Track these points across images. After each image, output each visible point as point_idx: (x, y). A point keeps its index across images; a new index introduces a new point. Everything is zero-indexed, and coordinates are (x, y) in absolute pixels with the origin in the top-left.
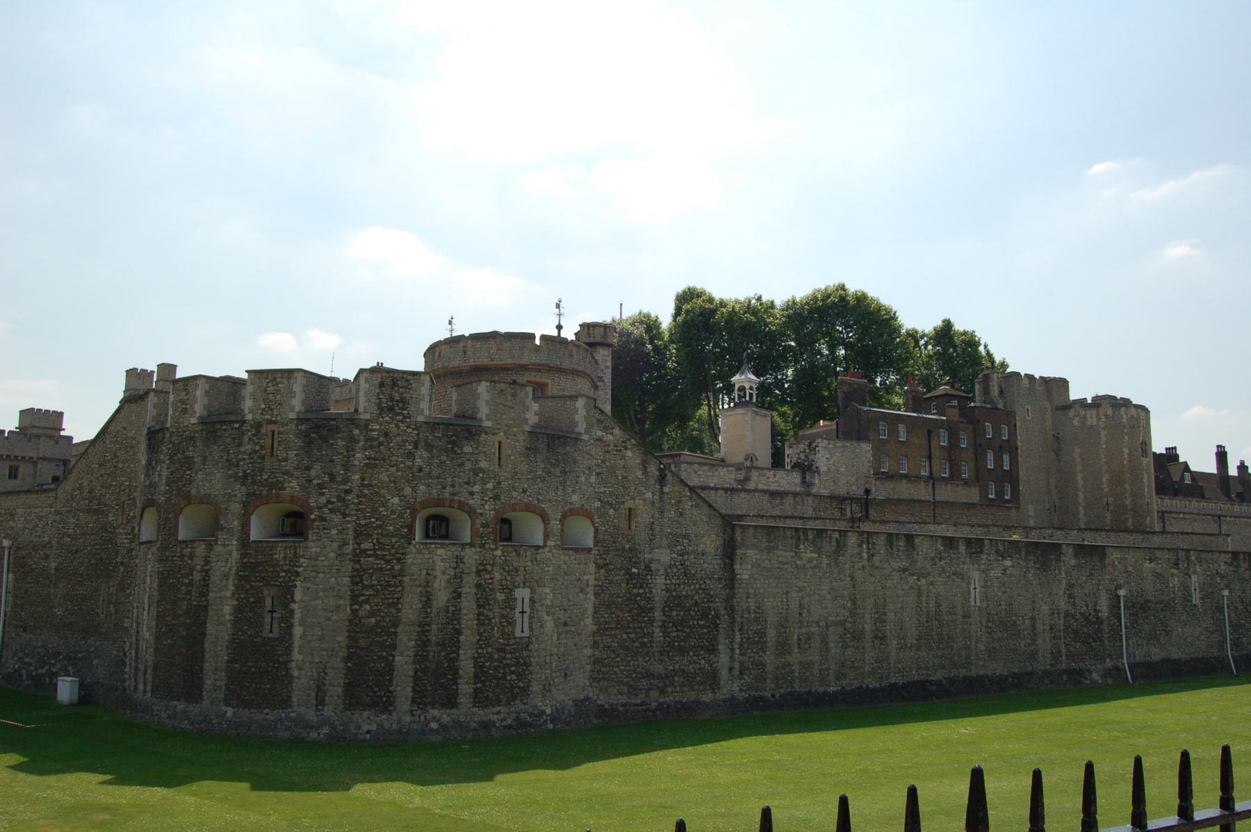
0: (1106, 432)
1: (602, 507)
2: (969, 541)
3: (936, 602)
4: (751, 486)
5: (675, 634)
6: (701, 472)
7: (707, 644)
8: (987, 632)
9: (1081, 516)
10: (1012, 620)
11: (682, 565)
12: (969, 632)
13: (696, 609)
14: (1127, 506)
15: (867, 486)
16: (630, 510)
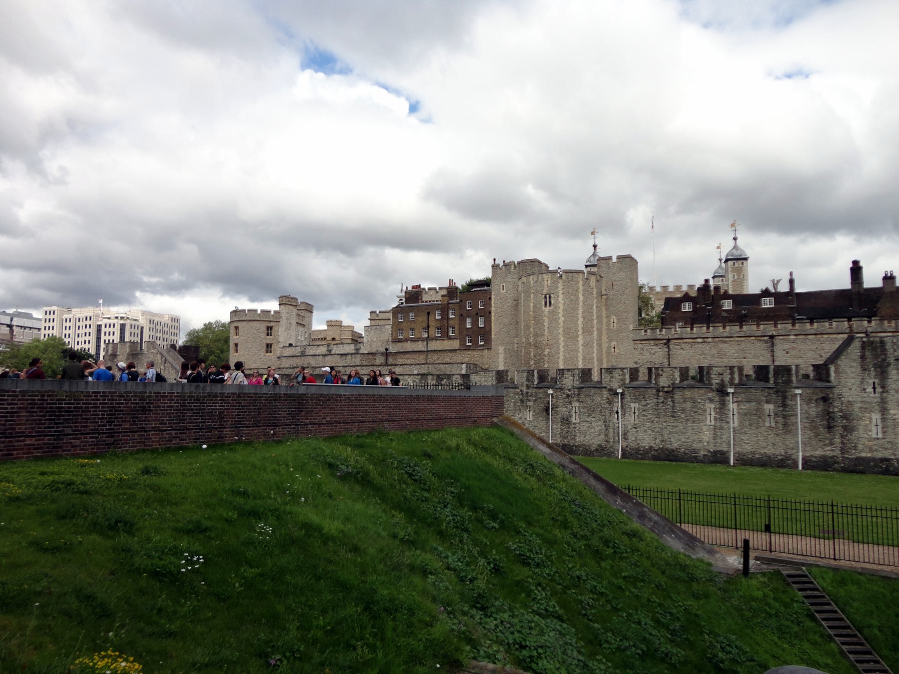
4: (333, 352)
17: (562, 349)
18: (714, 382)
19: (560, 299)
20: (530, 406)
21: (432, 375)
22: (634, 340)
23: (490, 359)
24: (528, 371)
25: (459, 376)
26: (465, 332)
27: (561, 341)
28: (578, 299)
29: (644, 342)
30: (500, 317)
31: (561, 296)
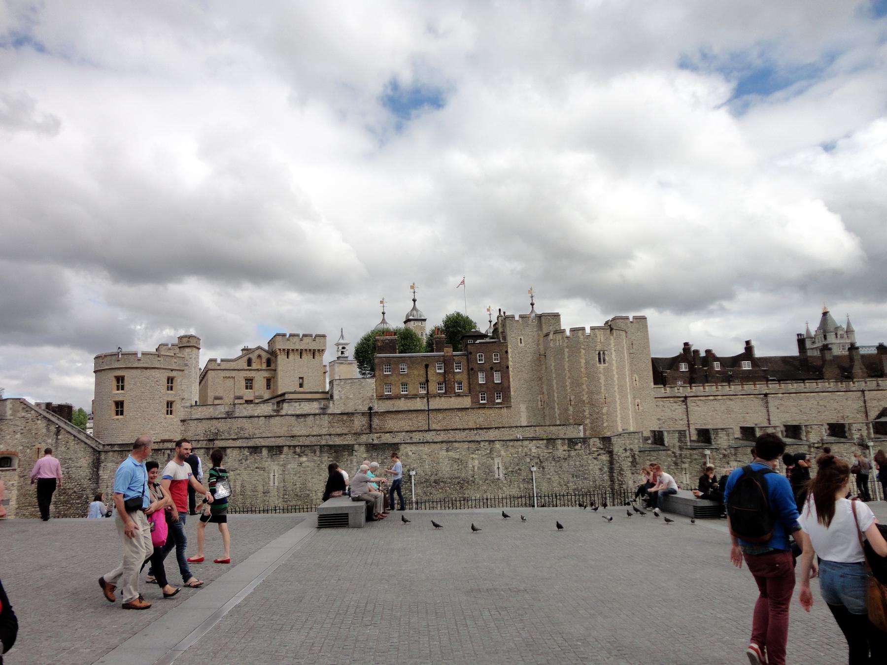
0: (568, 350)
1: (23, 449)
2: (270, 448)
3: (242, 485)
4: (283, 412)
5: (62, 508)
6: (249, 408)
7: (81, 512)
8: (283, 501)
9: (556, 410)
10: (305, 494)
11: (68, 473)
12: (268, 501)
13: (75, 494)
14: (584, 401)
15: (371, 405)
16: (38, 449)
17: (619, 408)
18: (855, 437)
19: (613, 356)
20: (685, 469)
21: (561, 439)
22: (656, 398)
23: (511, 418)
24: (680, 432)
25: (598, 439)
26: (478, 388)
27: (617, 399)
28: (624, 356)
29: (665, 399)
30: (519, 372)
31: (614, 353)
